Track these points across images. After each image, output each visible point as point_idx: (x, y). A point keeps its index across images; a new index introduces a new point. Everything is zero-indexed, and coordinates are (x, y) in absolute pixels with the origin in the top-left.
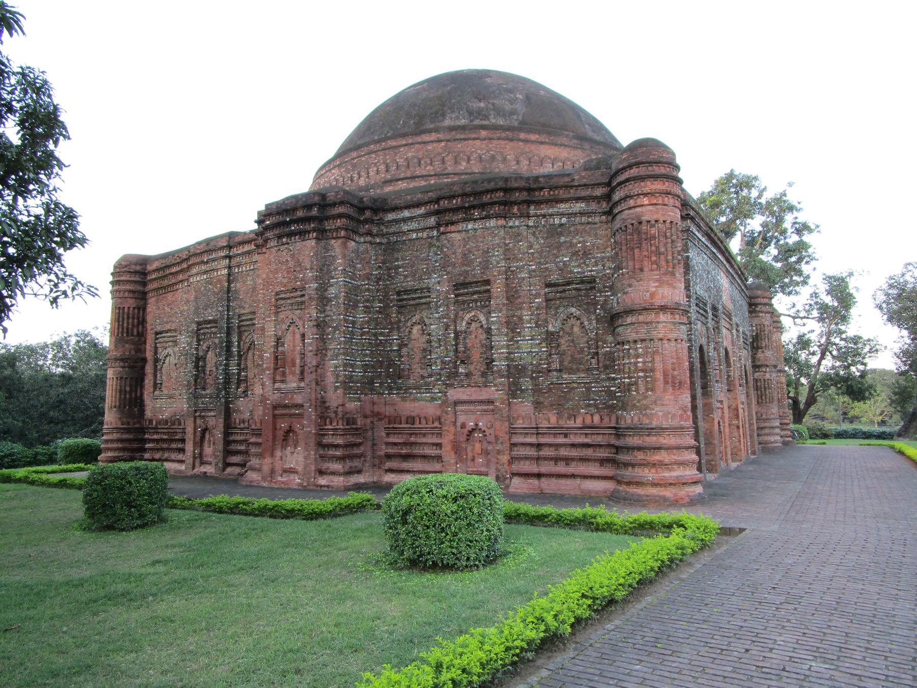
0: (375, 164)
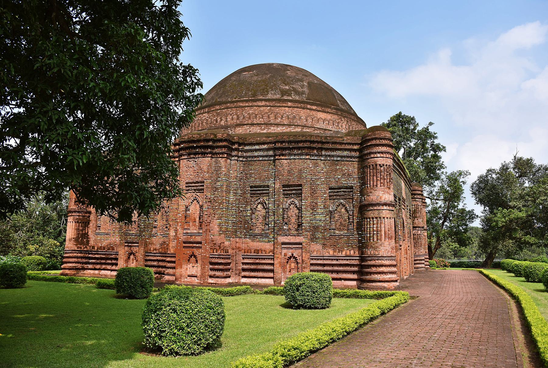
0: (231, 114)
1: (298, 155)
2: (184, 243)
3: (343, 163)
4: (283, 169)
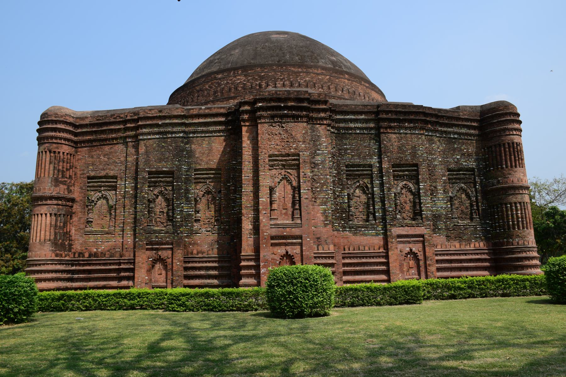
0: (281, 80)
1: (410, 128)
3: (461, 141)
4: (392, 145)
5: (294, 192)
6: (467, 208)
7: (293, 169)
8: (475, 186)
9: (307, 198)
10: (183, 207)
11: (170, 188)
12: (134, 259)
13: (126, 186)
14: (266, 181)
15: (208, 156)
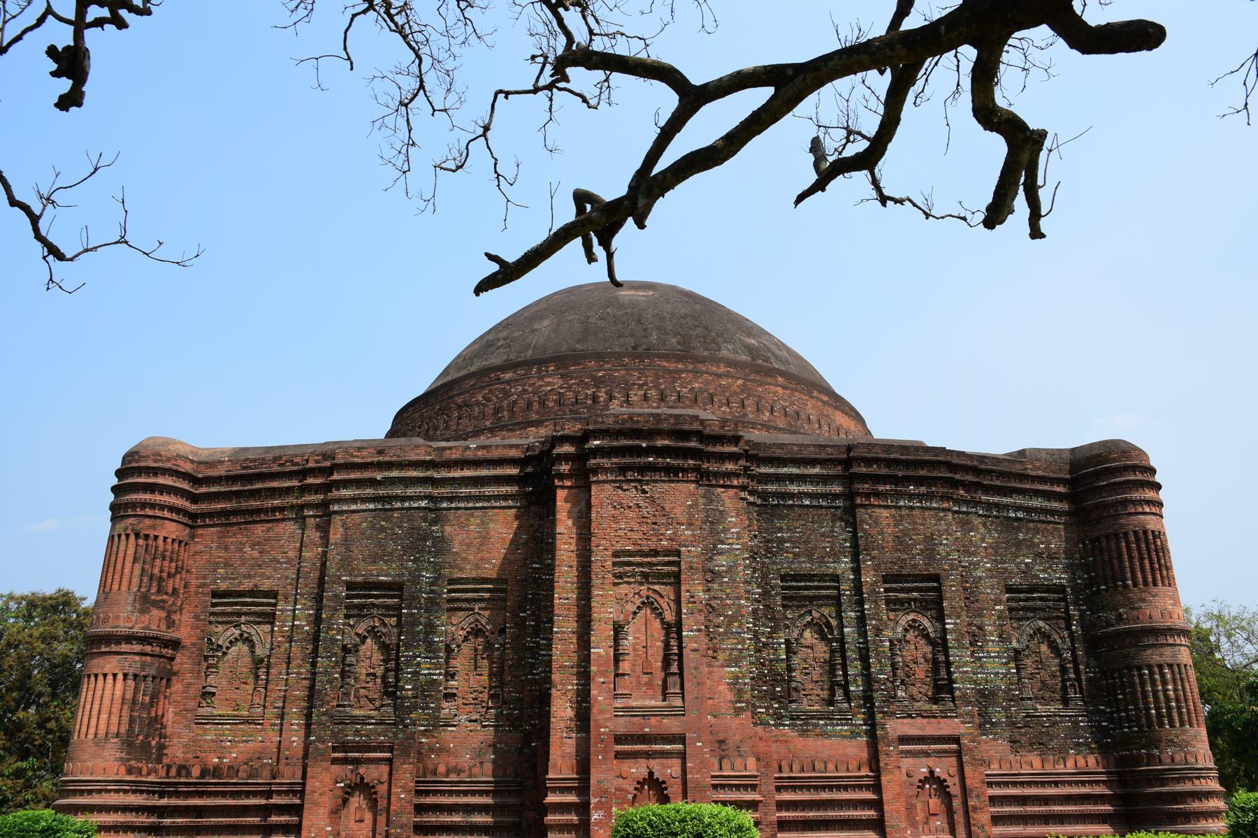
0: (641, 386)
1: (920, 497)
2: (619, 739)
3: (1031, 525)
4: (881, 533)
5: (667, 634)
6: (1053, 676)
7: (663, 584)
8: (1068, 627)
9: (695, 650)
10: (419, 664)
11: (393, 621)
12: (304, 784)
13: (295, 614)
14: (605, 611)
15: (479, 550)
